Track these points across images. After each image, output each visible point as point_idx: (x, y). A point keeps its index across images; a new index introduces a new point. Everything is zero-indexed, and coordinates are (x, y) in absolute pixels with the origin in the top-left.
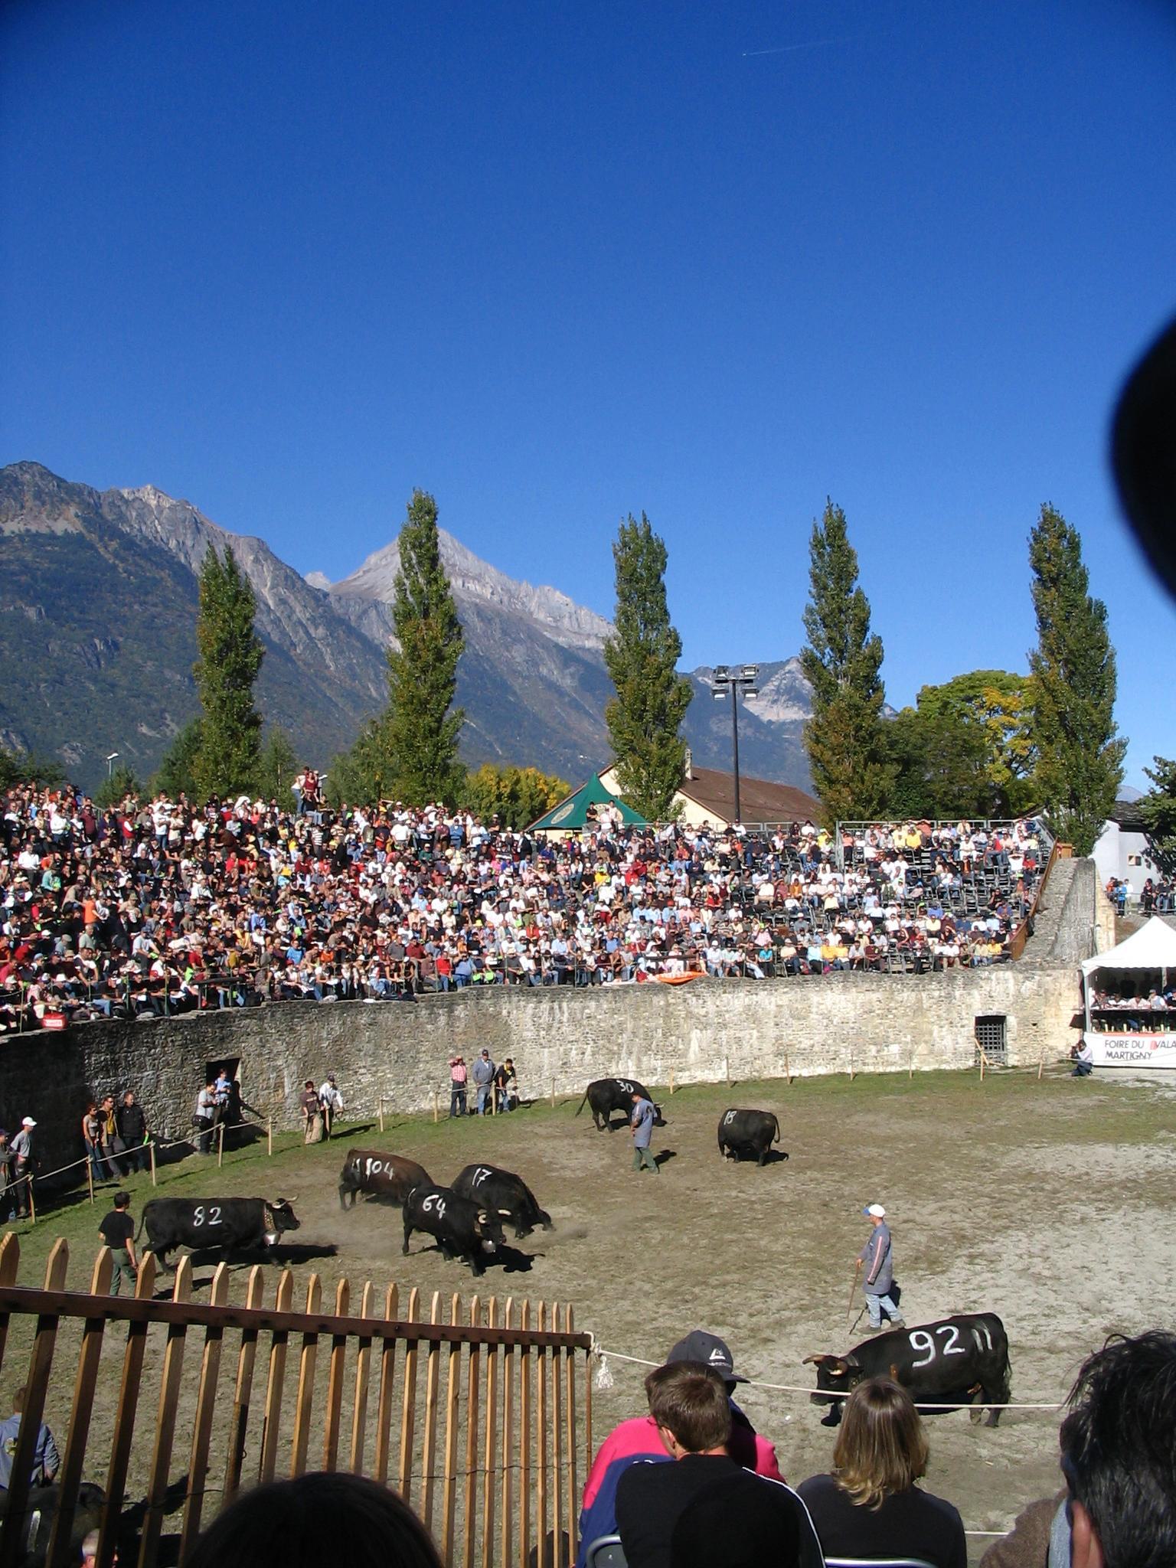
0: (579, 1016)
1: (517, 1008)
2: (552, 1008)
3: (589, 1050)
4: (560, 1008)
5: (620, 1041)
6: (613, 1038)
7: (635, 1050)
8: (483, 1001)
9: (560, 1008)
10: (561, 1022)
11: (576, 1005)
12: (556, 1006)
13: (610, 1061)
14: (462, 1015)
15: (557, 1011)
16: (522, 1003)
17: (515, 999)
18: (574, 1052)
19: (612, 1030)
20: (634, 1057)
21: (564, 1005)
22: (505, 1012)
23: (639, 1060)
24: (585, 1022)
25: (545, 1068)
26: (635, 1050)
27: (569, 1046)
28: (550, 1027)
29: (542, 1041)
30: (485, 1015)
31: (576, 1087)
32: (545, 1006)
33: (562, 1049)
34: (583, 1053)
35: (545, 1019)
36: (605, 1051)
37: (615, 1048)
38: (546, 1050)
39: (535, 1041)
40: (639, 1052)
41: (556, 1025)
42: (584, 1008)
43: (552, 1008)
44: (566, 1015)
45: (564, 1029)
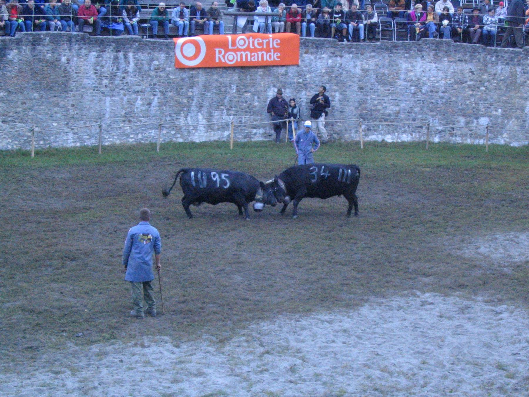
0: (146, 67)
1: (78, 56)
2: (116, 58)
3: (156, 101)
4: (126, 58)
5: (190, 94)
6: (184, 90)
7: (206, 104)
8: (40, 47)
9: (126, 58)
10: (126, 72)
11: (143, 56)
12: (121, 55)
13: (178, 114)
14: (16, 60)
15: (122, 61)
16: (83, 51)
17: (76, 47)
18: (139, 102)
19: (181, 83)
20: (205, 110)
21: (131, 55)
22: (64, 59)
23: (210, 115)
24: (152, 73)
25: (107, 116)
26: (206, 104)
27: (134, 96)
28: (113, 76)
29: (104, 89)
30: (40, 61)
31: (140, 136)
32: (109, 55)
33: (125, 99)
34: (149, 104)
35: (108, 67)
36: (172, 103)
37: (185, 101)
38: (108, 99)
39: (96, 89)
40: (210, 106)
41: (120, 74)
42: (152, 60)
43: (116, 58)
44: (132, 65)
45: (129, 79)
